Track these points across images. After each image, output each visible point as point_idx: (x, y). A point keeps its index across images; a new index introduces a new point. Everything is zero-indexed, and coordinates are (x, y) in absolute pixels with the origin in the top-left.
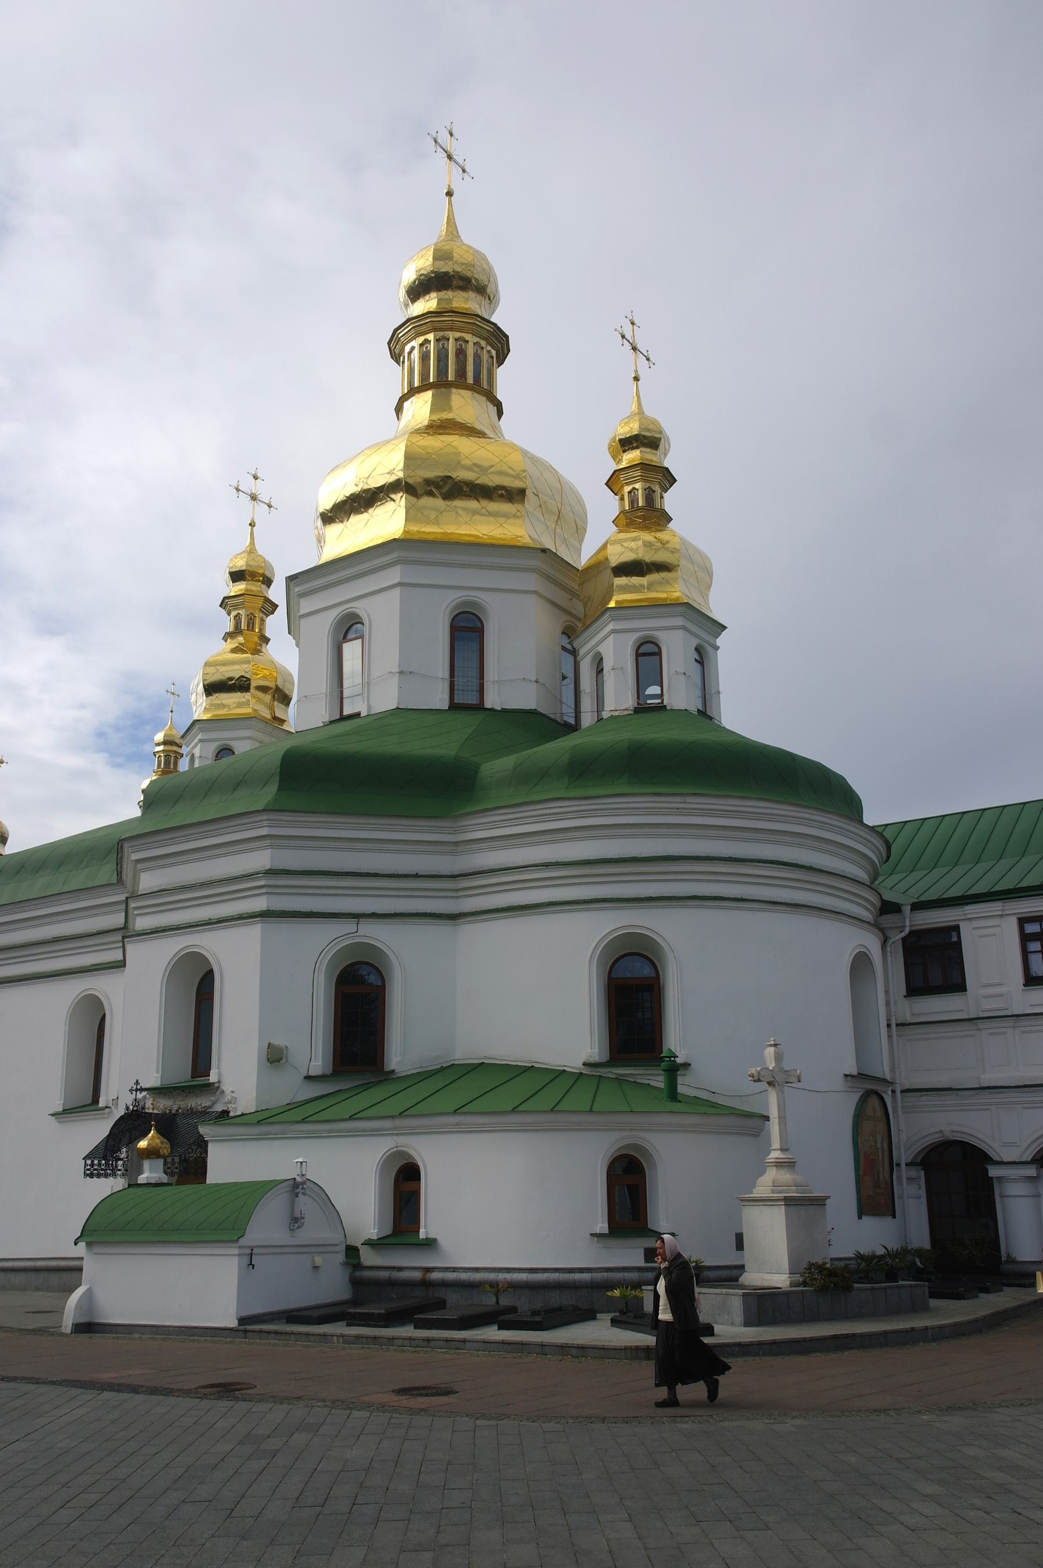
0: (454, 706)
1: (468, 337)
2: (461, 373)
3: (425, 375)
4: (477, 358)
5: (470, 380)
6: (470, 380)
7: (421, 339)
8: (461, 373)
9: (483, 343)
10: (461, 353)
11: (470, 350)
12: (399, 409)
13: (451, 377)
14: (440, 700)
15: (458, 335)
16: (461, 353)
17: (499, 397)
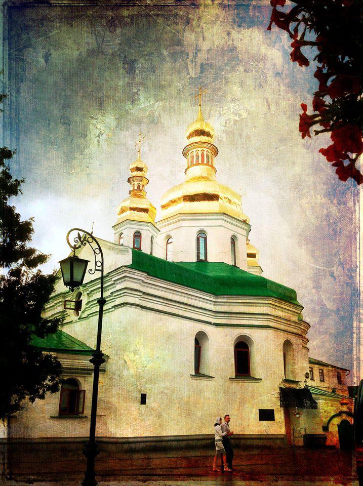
1: (204, 149)
2: (203, 161)
3: (192, 162)
5: (205, 162)
6: (205, 162)
7: (191, 151)
8: (203, 161)
9: (209, 151)
10: (203, 155)
11: (205, 153)
12: (185, 172)
13: (200, 162)
14: (195, 260)
15: (202, 149)
16: (203, 155)
17: (214, 165)
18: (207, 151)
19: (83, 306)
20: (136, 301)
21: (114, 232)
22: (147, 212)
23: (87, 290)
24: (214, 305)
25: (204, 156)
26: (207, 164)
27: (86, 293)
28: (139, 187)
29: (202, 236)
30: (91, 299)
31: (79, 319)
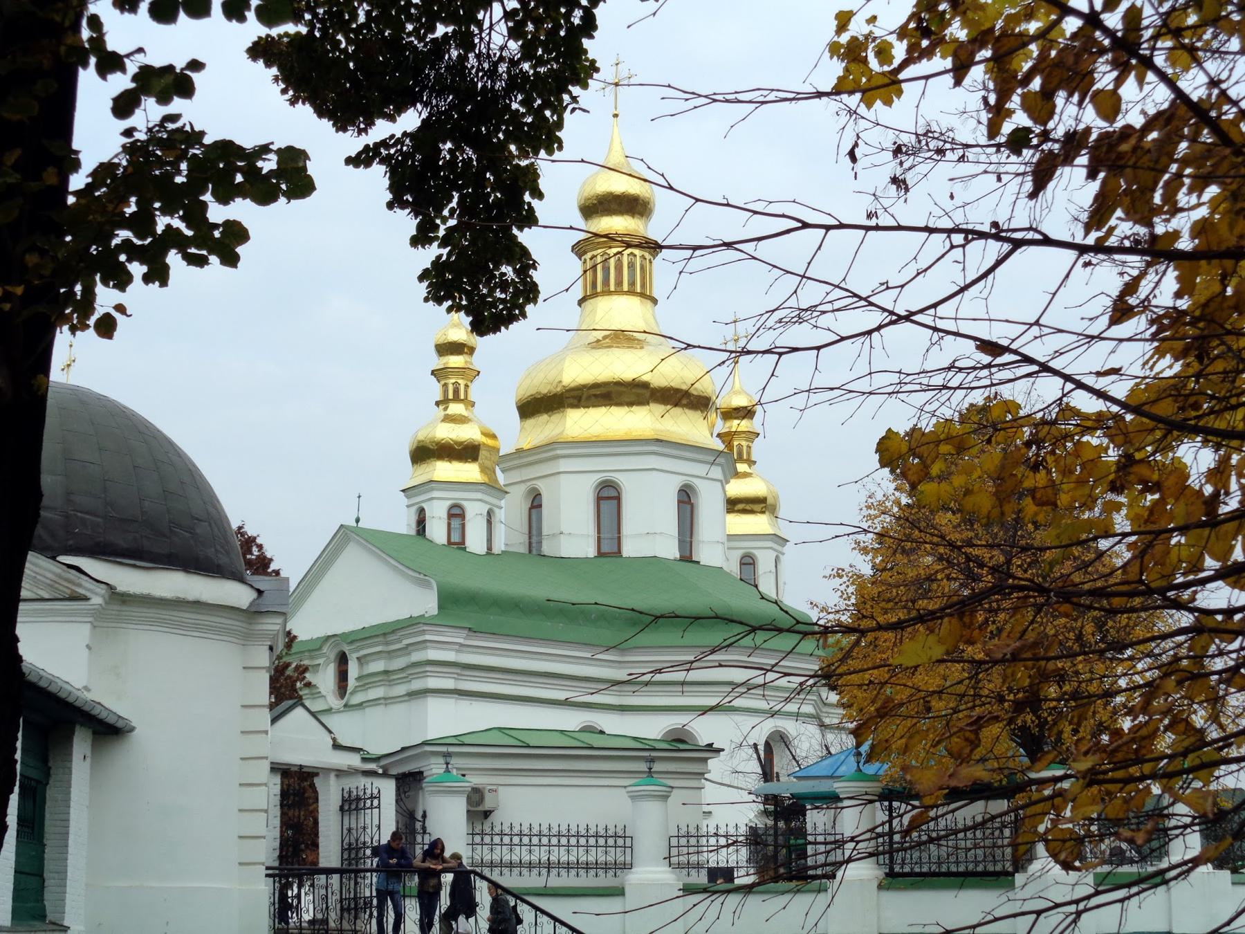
0: (601, 554)
2: (619, 283)
4: (631, 266)
5: (626, 288)
6: (626, 288)
7: (589, 255)
8: (619, 283)
14: (591, 552)
18: (632, 253)
19: (352, 682)
20: (449, 684)
21: (405, 501)
22: (474, 458)
23: (357, 650)
24: (620, 668)
25: (621, 267)
26: (631, 292)
27: (355, 655)
28: (456, 391)
29: (608, 497)
30: (366, 672)
31: (345, 706)
